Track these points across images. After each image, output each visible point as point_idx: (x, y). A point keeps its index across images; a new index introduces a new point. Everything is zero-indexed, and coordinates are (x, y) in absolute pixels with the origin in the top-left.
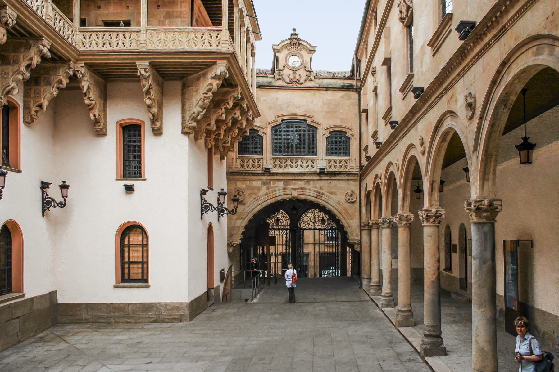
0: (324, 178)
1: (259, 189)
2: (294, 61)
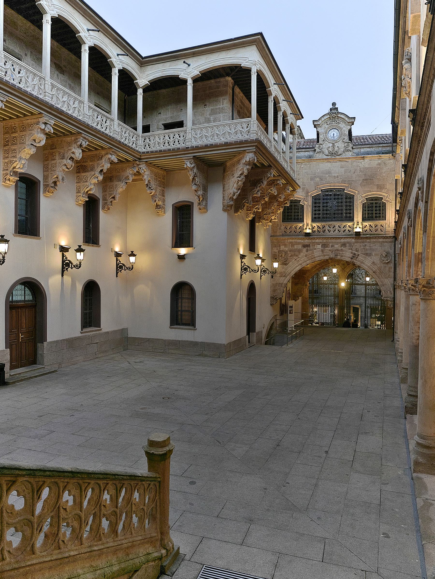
1: (300, 251)
2: (334, 134)
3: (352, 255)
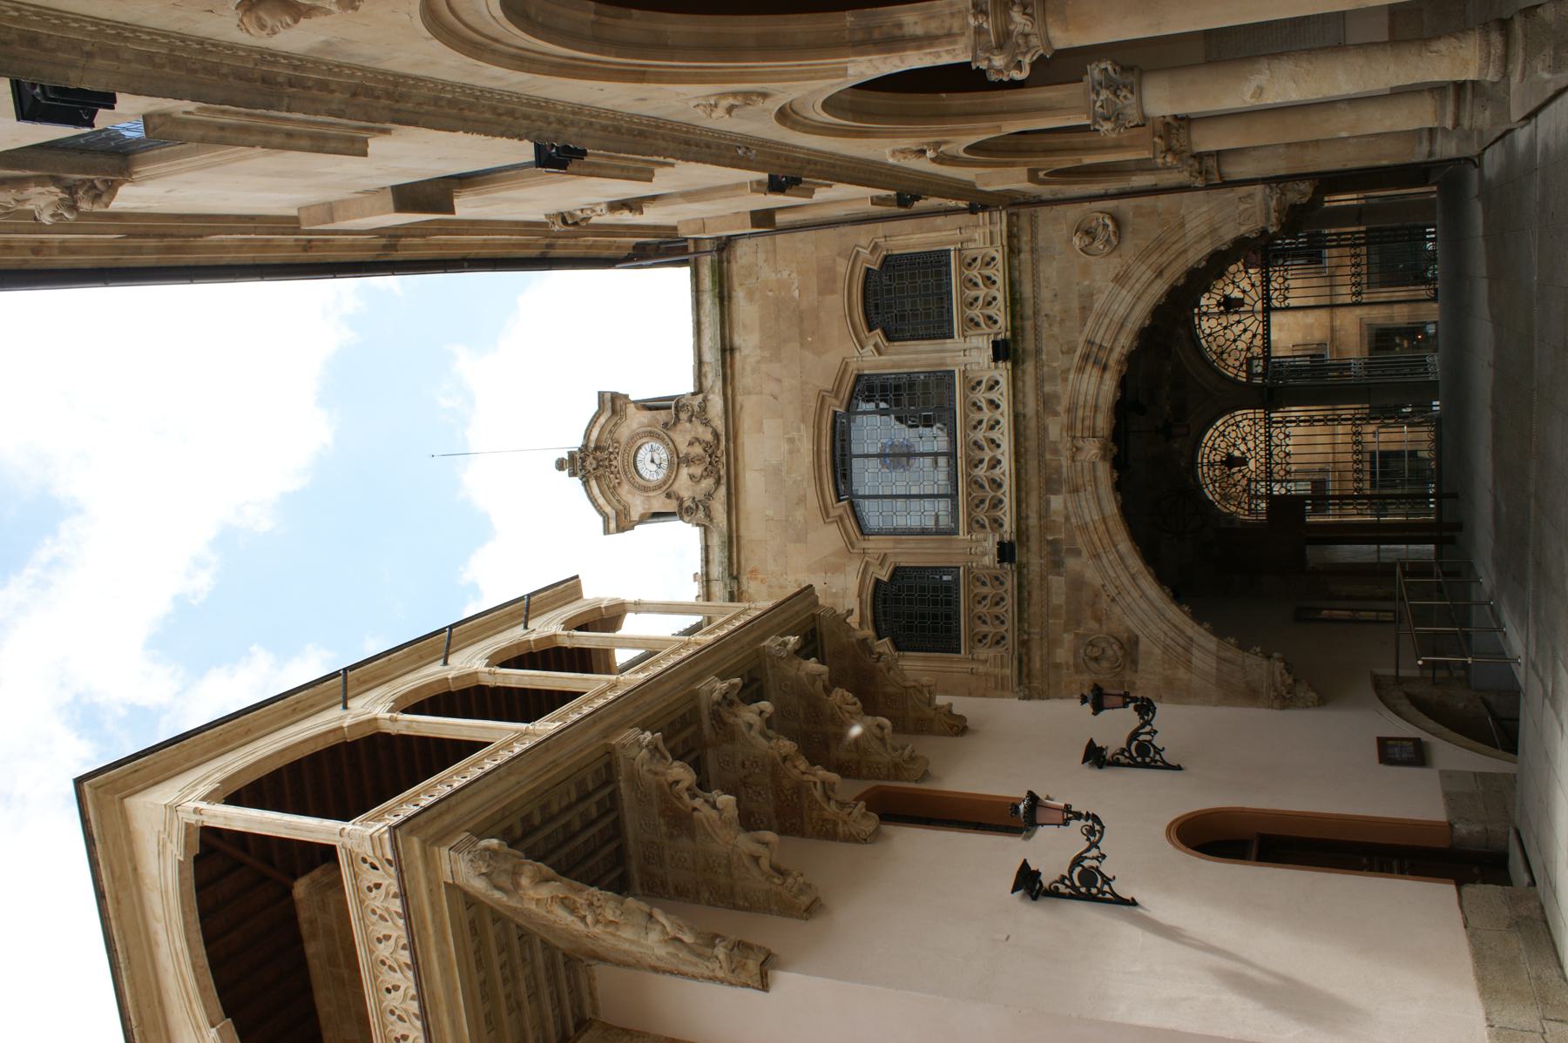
0: (1029, 344)
1: (1077, 584)
2: (651, 461)
3: (1089, 368)
